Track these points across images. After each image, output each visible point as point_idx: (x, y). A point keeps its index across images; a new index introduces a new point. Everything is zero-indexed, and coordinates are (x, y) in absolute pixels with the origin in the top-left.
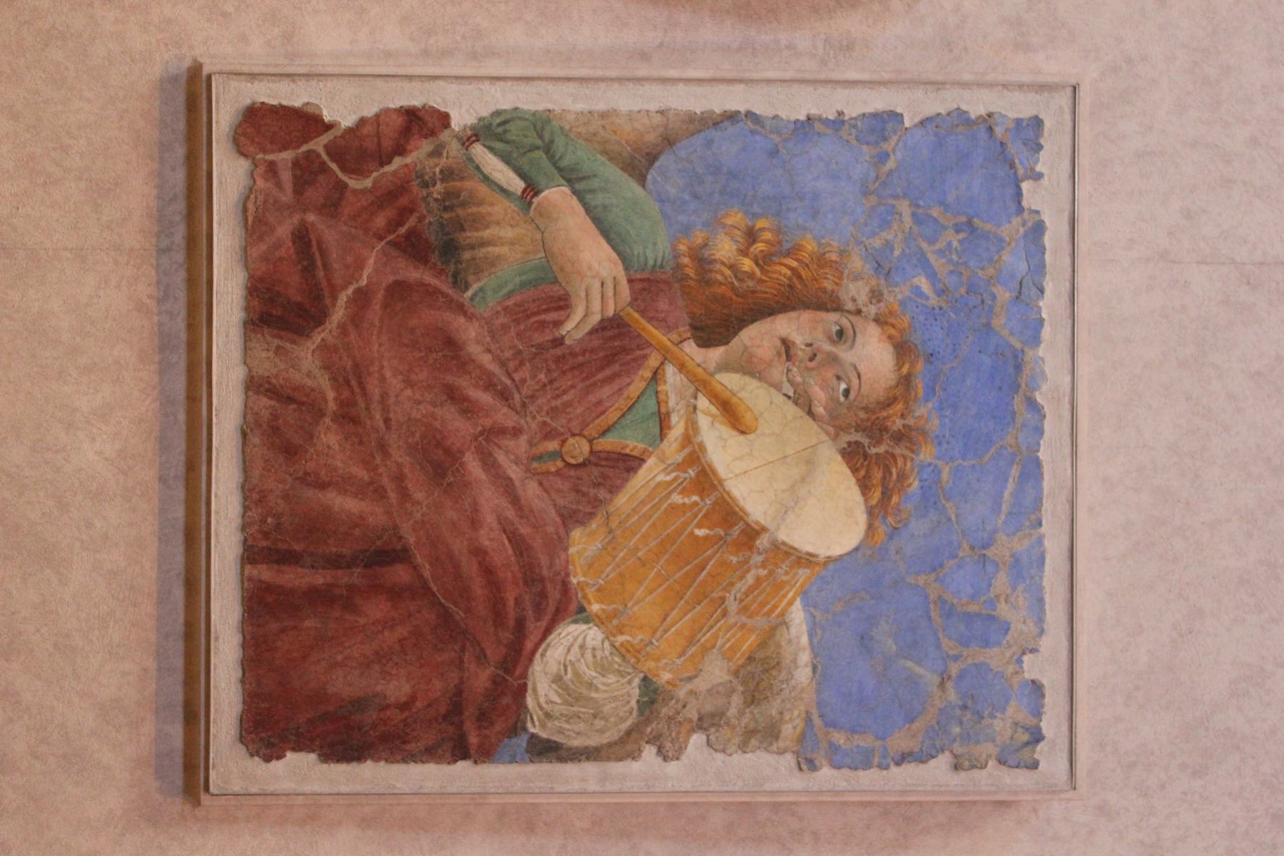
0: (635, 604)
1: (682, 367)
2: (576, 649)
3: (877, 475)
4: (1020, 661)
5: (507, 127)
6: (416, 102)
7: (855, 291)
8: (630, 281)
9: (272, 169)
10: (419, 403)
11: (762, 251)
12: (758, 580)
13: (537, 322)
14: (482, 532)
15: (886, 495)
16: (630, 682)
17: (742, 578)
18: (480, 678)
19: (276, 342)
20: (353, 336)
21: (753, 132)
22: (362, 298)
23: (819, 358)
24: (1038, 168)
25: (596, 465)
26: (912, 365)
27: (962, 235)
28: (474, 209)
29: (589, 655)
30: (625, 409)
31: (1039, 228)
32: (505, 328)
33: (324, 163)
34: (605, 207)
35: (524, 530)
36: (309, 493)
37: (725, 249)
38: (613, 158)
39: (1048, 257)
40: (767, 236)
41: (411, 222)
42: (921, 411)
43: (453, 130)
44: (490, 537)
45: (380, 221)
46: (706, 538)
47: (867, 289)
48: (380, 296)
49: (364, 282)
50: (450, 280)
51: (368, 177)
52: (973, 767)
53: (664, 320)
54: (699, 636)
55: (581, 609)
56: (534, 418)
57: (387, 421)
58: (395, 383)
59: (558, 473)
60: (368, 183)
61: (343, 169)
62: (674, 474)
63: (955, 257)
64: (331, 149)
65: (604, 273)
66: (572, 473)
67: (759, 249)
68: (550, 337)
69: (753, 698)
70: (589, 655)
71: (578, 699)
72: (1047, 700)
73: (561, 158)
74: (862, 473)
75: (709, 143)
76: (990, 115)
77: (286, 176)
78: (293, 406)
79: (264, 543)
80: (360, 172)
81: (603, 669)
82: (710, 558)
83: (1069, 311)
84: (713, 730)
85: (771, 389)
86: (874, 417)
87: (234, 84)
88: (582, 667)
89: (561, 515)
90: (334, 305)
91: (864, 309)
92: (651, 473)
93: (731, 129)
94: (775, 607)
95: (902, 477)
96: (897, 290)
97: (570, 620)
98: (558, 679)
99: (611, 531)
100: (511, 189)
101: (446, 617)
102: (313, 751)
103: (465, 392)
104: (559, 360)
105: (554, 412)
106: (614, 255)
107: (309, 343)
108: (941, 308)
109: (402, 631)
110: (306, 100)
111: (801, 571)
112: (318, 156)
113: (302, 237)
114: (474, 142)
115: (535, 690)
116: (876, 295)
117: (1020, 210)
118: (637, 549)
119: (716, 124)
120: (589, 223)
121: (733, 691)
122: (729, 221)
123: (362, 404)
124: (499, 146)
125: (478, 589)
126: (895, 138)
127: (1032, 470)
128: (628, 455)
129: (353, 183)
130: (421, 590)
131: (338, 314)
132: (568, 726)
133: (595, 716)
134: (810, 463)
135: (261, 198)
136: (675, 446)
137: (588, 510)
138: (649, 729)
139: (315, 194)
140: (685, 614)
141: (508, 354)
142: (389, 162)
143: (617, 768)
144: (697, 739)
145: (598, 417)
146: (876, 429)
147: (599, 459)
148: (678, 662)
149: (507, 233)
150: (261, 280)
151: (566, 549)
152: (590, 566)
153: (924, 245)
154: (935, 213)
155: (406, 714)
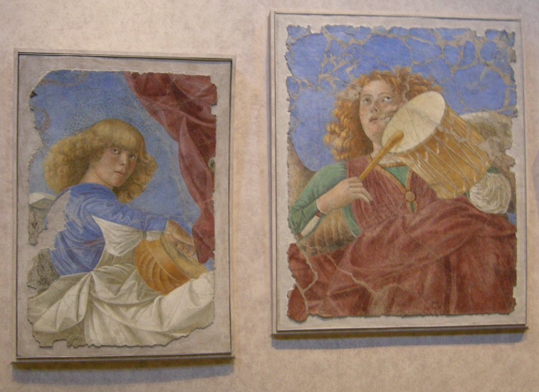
0: (463, 175)
1: (380, 158)
2: (478, 196)
3: (417, 87)
4: (479, 38)
5: (295, 222)
6: (286, 256)
7: (352, 94)
8: (350, 176)
9: (311, 308)
10: (394, 254)
11: (338, 128)
12: (454, 130)
13: (365, 211)
14: (439, 230)
15: (424, 84)
16: (489, 177)
17: (453, 136)
18: (488, 230)
19: (373, 305)
20: (371, 278)
21: (295, 132)
22: (357, 274)
23: (376, 108)
24: (306, 27)
25: (415, 189)
26: (378, 74)
27: (331, 55)
28: (325, 234)
29: (481, 191)
30: (395, 178)
31: (328, 27)
32: (367, 223)
33: (309, 290)
34: (324, 186)
35: (438, 215)
36: (426, 292)
37: (338, 142)
38: (305, 183)
39: (338, 24)
40: (333, 127)
41: (330, 257)
42: (394, 71)
43: (297, 242)
44: (440, 227)
45: (329, 268)
46: (440, 149)
47: (351, 90)
48: (356, 268)
49: (351, 274)
50: (350, 243)
51: (314, 273)
52: (515, 55)
53: (364, 164)
54: (473, 152)
55: (465, 194)
56: (399, 212)
57: (400, 265)
58: (387, 262)
59: (418, 203)
60: (316, 273)
61: (310, 282)
62: (418, 161)
63: (339, 58)
64: (304, 287)
65: (347, 187)
66: (418, 197)
67: (338, 129)
68: (370, 207)
69: (494, 133)
70: (481, 191)
71: (495, 195)
72: (492, 28)
73: (306, 202)
74: (416, 93)
75: (300, 148)
76: (287, 44)
77: (314, 303)
78: (395, 298)
79: (442, 308)
80: (312, 276)
81: (484, 187)
82: (446, 147)
83: (357, 17)
84: (505, 147)
85: (388, 125)
86: (397, 88)
87: (281, 322)
88: (485, 193)
89: (433, 201)
90: (359, 285)
91: (358, 91)
92: (418, 169)
93: (295, 140)
94: (463, 124)
95: (417, 78)
96: (351, 79)
97: (468, 198)
98: (489, 202)
99: (438, 184)
100: (317, 221)
101: (468, 243)
102: (513, 288)
103: (390, 237)
104: (378, 203)
105: (397, 205)
106: (341, 183)
107: (373, 293)
108: (357, 63)
109: (472, 258)
110: (286, 297)
111: (451, 115)
112: (307, 291)
113: (336, 297)
114: (301, 235)
115: (493, 210)
116: (353, 87)
117: (322, 34)
118: (444, 174)
119: (293, 145)
120: (330, 192)
121: (492, 140)
122: (328, 140)
123: (395, 274)
124: (302, 225)
125: (458, 231)
126: (297, 79)
127: (413, 31)
128: (412, 177)
129: (316, 278)
130: (459, 251)
131: (363, 283)
132: (504, 198)
133: (501, 189)
134: (413, 112)
135: (322, 312)
136: (408, 160)
137: (431, 191)
138: (505, 170)
139: (320, 292)
140: (466, 157)
141: (376, 221)
142: (308, 266)
143: (517, 182)
144: (508, 153)
145: (398, 189)
146: (401, 87)
147: (413, 189)
148: (482, 159)
149: (333, 222)
150: (351, 311)
151: (444, 200)
152: (450, 191)
153: (335, 69)
154: (323, 65)
155: (500, 256)
